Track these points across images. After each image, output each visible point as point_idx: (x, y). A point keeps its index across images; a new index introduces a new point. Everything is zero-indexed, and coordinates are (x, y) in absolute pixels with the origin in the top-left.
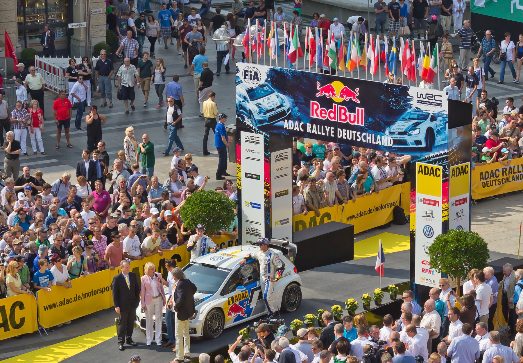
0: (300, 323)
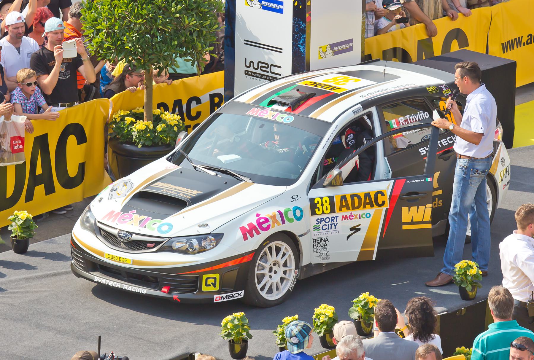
0: (375, 302)
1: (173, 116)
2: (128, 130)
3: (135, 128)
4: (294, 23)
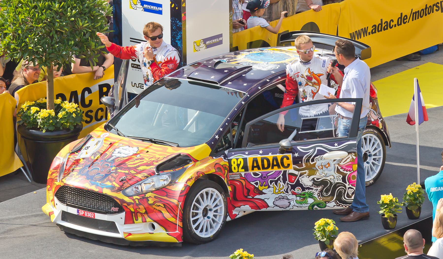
1: (72, 104)
2: (33, 118)
3: (39, 116)
4: (171, 22)
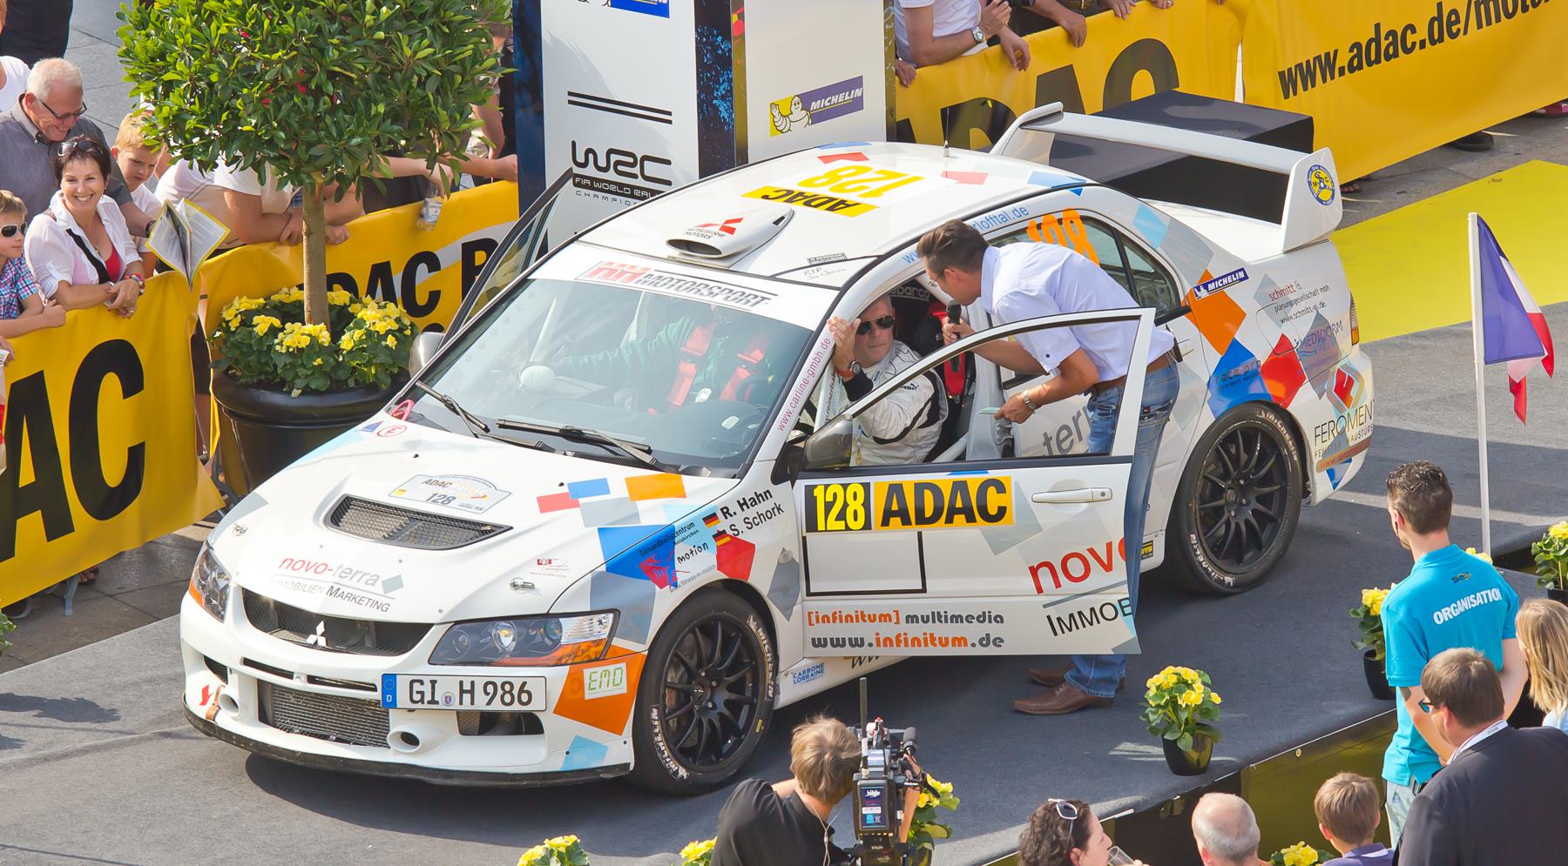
4: (698, 42)
